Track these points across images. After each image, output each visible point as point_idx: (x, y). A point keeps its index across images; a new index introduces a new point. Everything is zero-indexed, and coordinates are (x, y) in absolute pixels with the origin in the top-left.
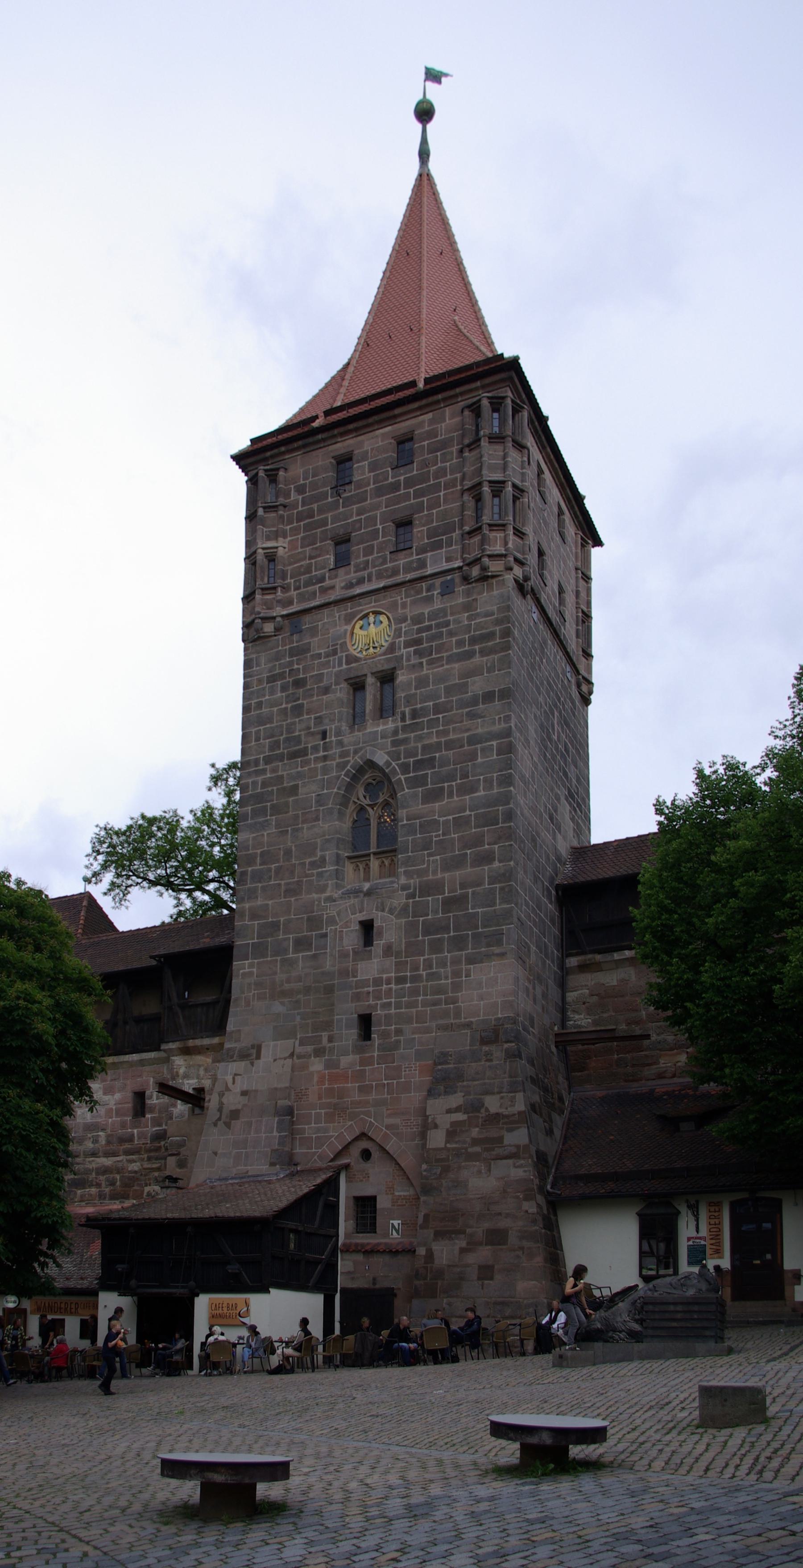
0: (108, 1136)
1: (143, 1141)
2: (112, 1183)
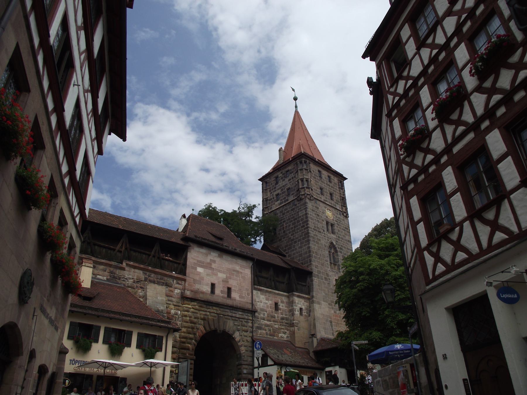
0: (268, 314)
2: (270, 331)
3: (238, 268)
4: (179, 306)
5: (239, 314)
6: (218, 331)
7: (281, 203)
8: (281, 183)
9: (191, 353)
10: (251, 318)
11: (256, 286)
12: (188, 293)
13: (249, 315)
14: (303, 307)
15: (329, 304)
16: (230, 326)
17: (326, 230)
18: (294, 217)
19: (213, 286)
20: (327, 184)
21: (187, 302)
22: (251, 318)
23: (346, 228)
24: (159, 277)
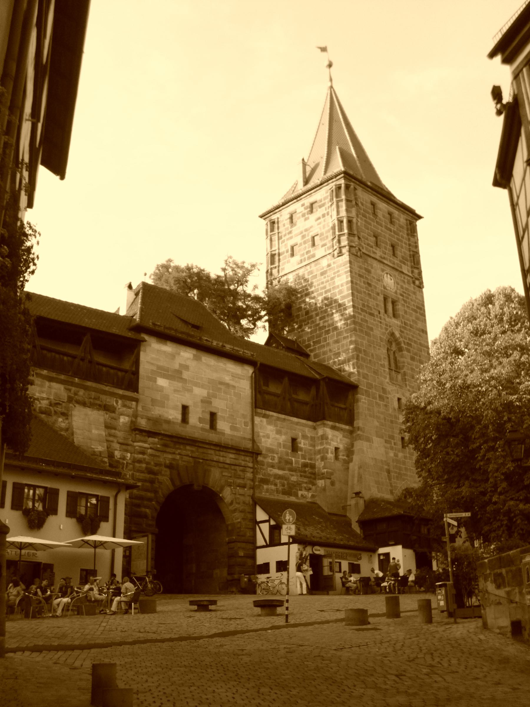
0: (280, 458)
1: (297, 466)
3: (227, 379)
4: (127, 445)
5: (230, 457)
6: (196, 487)
7: (301, 261)
8: (301, 224)
9: (150, 522)
10: (251, 465)
11: (259, 410)
12: (143, 423)
13: (248, 459)
14: (341, 447)
15: (386, 442)
16: (215, 477)
17: (382, 311)
18: (325, 287)
19: (185, 409)
20: (386, 228)
21: (142, 438)
22: (251, 465)
23: (418, 307)
24: (93, 394)
